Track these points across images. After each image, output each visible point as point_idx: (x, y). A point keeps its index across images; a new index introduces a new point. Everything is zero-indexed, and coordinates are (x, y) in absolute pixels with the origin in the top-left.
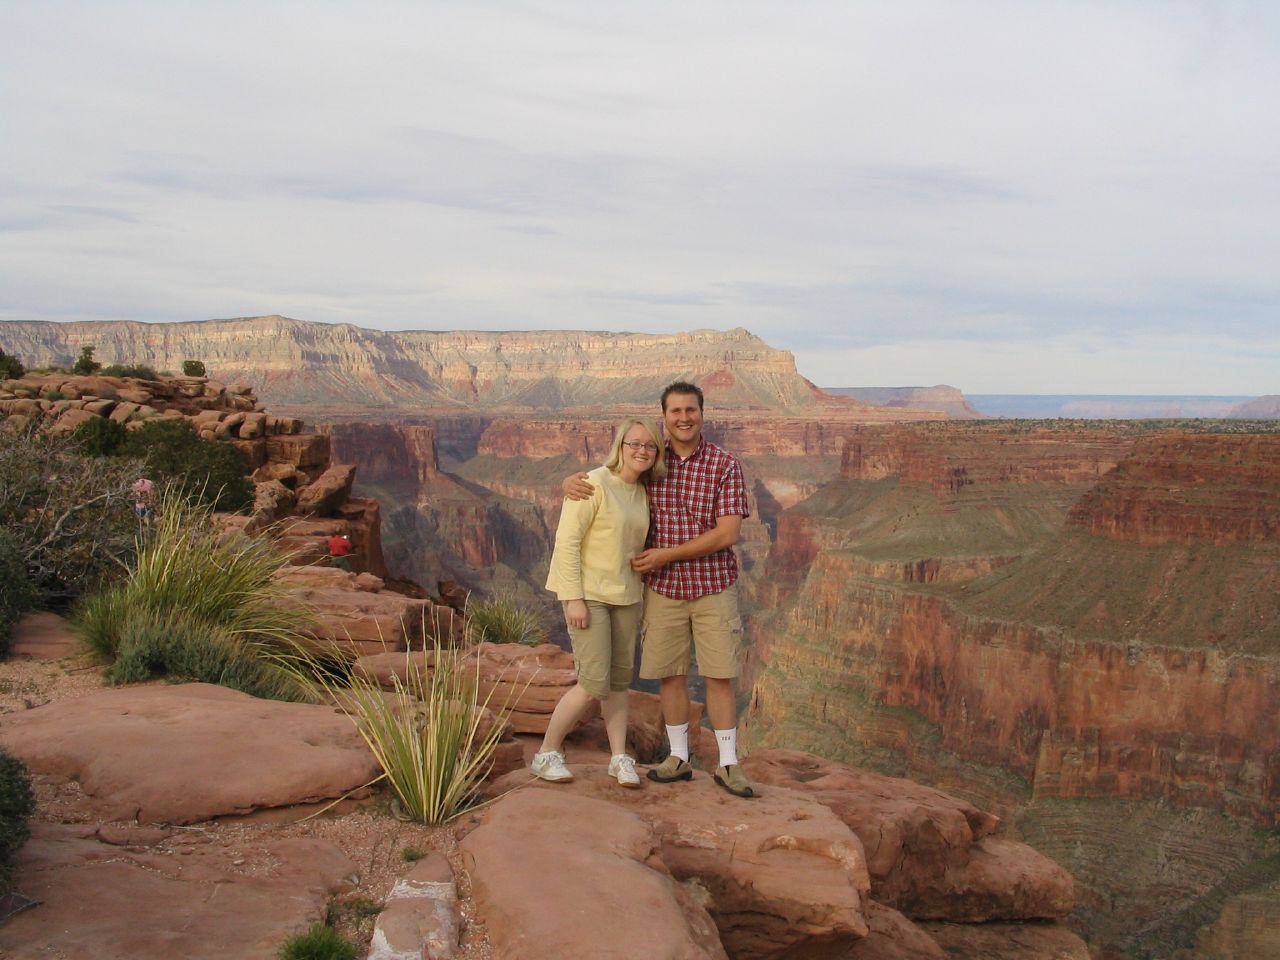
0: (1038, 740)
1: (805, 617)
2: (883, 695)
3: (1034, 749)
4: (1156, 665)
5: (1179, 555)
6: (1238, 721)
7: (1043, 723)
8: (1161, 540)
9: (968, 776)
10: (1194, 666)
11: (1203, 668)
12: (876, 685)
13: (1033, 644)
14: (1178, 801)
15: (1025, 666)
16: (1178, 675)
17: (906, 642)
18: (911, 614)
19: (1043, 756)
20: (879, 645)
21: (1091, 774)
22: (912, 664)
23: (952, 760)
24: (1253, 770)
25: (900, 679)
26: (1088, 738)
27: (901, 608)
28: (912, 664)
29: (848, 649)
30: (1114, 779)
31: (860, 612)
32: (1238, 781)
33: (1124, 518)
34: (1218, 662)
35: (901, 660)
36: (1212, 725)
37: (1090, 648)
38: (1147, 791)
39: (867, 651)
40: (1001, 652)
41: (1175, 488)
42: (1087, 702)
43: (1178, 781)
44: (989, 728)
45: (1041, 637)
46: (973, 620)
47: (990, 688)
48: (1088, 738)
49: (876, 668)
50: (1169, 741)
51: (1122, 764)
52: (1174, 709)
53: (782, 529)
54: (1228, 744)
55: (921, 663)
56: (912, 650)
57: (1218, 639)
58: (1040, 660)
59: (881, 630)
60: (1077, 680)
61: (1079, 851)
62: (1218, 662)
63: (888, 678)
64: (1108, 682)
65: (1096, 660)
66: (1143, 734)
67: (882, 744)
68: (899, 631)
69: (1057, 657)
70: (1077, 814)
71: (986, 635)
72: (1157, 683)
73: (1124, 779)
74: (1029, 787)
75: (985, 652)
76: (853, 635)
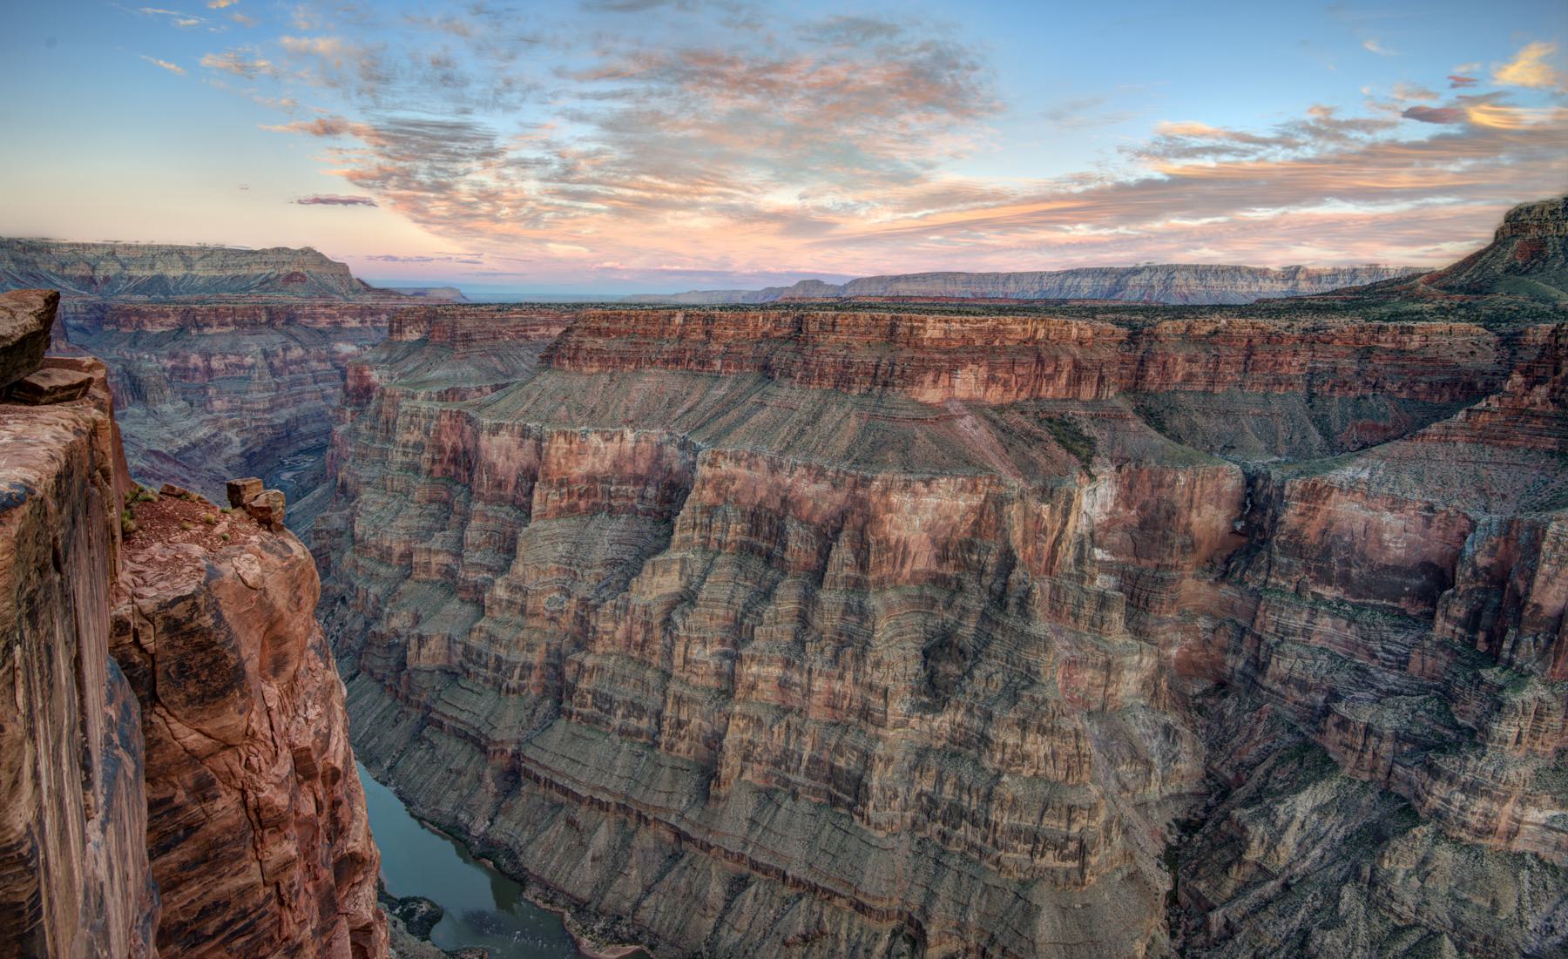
0: (532, 488)
1: (372, 428)
2: (431, 471)
3: (530, 493)
4: (595, 440)
5: (605, 379)
6: (642, 466)
7: (534, 478)
8: (594, 370)
9: (490, 514)
10: (617, 439)
11: (622, 439)
12: (426, 466)
13: (525, 433)
14: (612, 511)
15: (520, 446)
16: (609, 444)
17: (443, 438)
18: (445, 421)
19: (536, 498)
20: (426, 441)
21: (564, 504)
22: (448, 450)
23: (479, 506)
24: (651, 491)
25: (441, 461)
26: (561, 484)
27: (438, 418)
28: (448, 450)
29: (405, 446)
30: (577, 505)
31: (411, 422)
32: (643, 498)
33: (573, 359)
34: (630, 435)
35: (441, 450)
36: (629, 469)
37: (559, 434)
38: (594, 510)
39: (419, 446)
40: (504, 438)
41: (601, 341)
42: (559, 463)
43: (613, 502)
44: (500, 485)
45: (529, 430)
46: (487, 422)
47: (500, 462)
48: (561, 484)
49: (426, 455)
50: (606, 480)
51: (580, 496)
52: (607, 463)
53: (351, 373)
54: (637, 479)
55: (454, 450)
56: (448, 444)
57: (628, 422)
58: (529, 443)
59: (427, 433)
60: (553, 452)
61: (560, 548)
62: (630, 435)
63: (434, 461)
64: (570, 451)
65: (562, 439)
66: (591, 478)
67: (430, 501)
68: (439, 432)
69: (540, 440)
70: (557, 527)
71: (495, 430)
72: (597, 449)
73: (582, 504)
74: (529, 515)
75: (495, 440)
76: (407, 436)
